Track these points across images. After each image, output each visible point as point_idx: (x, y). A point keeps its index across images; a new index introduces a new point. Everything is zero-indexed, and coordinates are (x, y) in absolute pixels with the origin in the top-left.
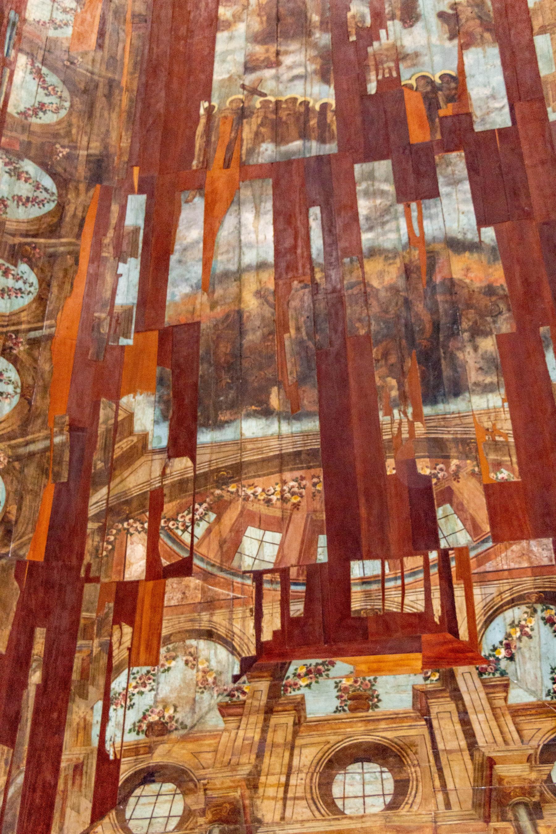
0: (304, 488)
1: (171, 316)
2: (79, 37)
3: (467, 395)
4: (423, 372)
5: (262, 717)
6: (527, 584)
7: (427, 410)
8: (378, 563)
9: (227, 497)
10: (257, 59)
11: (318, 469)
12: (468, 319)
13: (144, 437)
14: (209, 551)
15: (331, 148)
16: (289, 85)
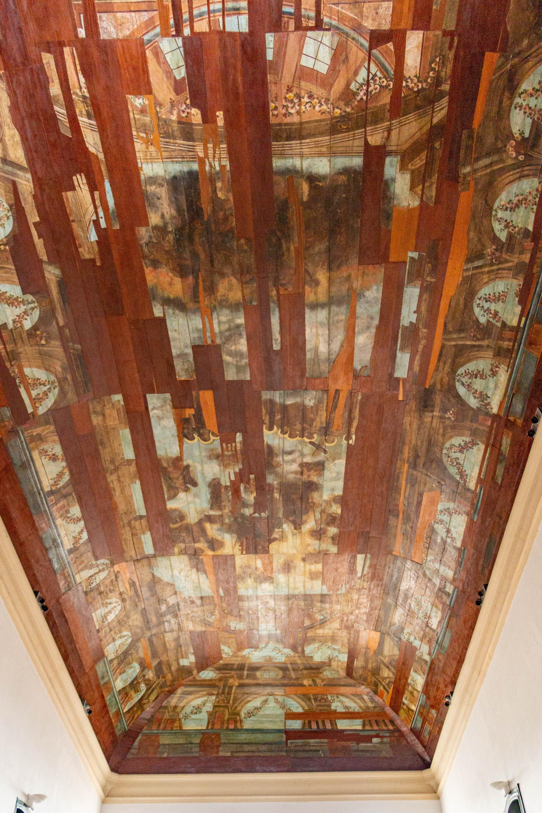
0: (284, 106)
1: (380, 273)
2: (434, 502)
3: (167, 177)
4: (199, 199)
7: (195, 167)
8: (228, 29)
9: (342, 104)
10: (315, 471)
11: (273, 122)
12: (169, 242)
13: (403, 167)
14: (357, 54)
15: (266, 395)
16: (294, 448)
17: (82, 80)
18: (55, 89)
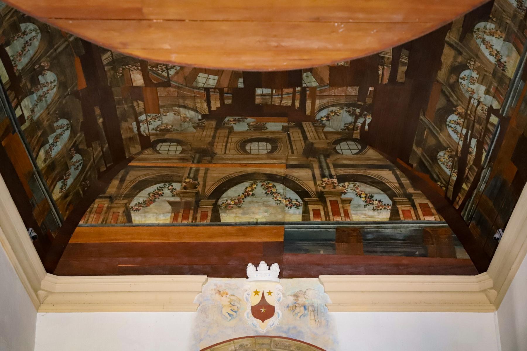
5: (213, 130)
6: (343, 100)
17: (380, 72)
18: (402, 69)
